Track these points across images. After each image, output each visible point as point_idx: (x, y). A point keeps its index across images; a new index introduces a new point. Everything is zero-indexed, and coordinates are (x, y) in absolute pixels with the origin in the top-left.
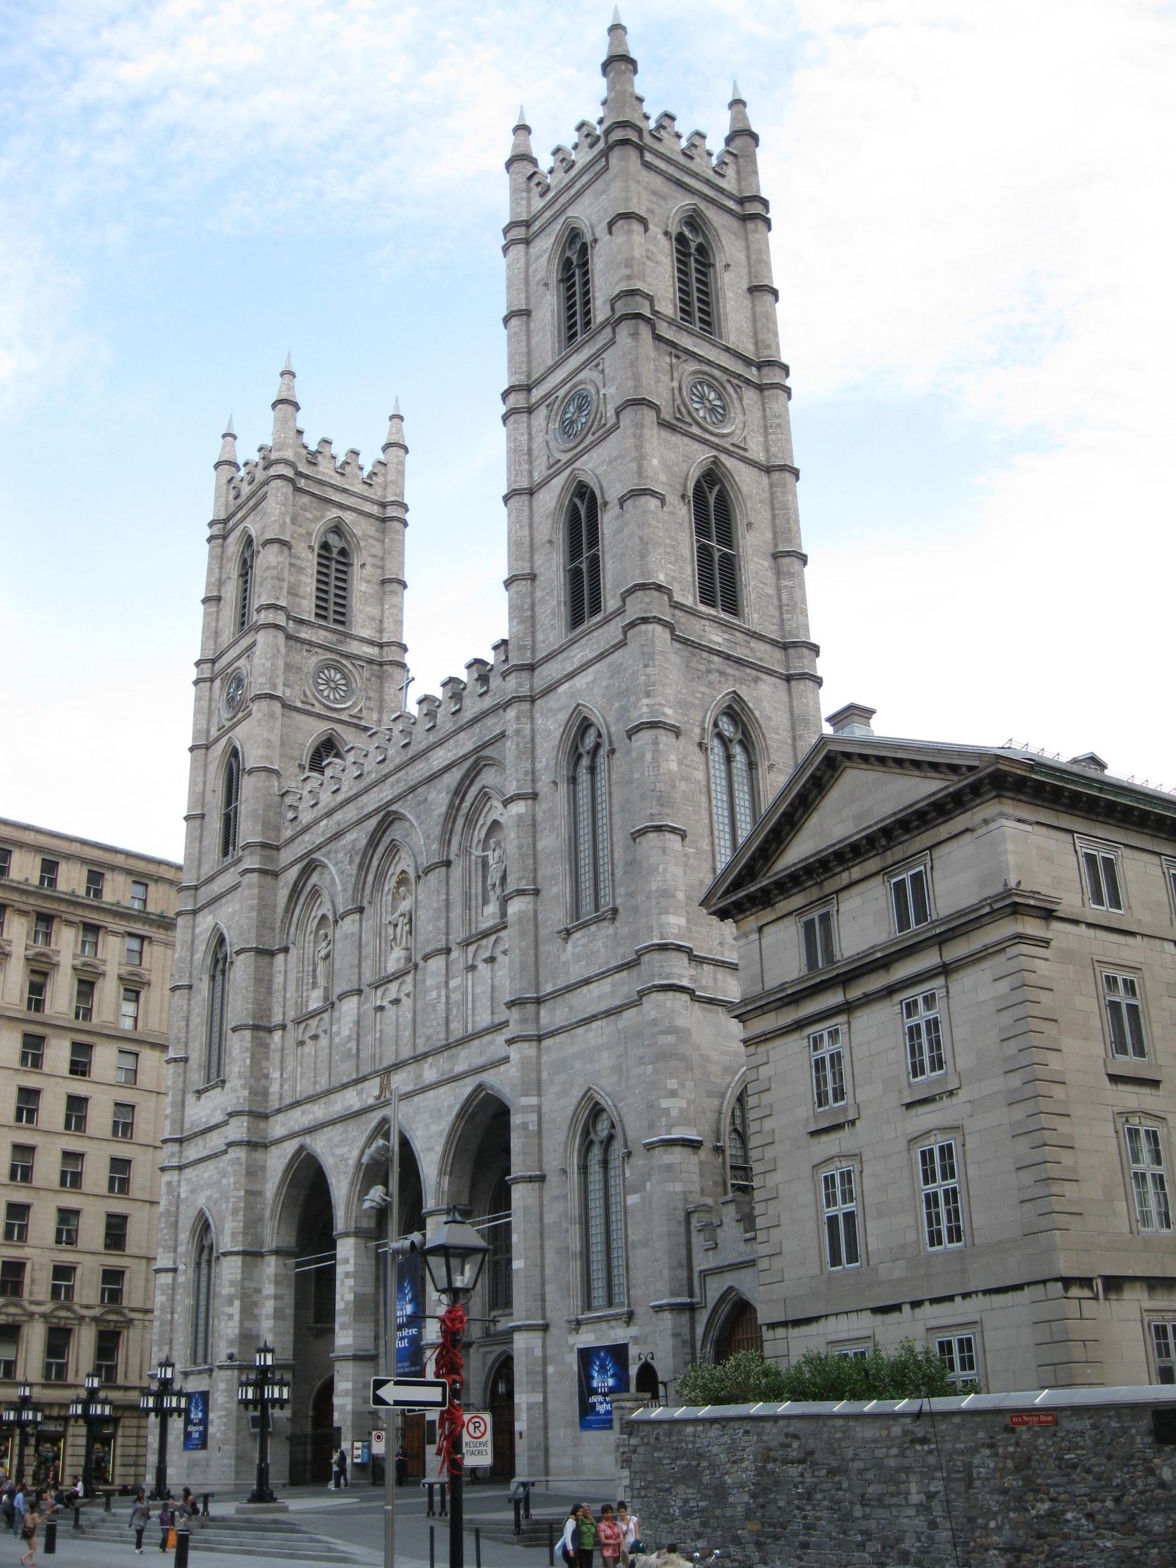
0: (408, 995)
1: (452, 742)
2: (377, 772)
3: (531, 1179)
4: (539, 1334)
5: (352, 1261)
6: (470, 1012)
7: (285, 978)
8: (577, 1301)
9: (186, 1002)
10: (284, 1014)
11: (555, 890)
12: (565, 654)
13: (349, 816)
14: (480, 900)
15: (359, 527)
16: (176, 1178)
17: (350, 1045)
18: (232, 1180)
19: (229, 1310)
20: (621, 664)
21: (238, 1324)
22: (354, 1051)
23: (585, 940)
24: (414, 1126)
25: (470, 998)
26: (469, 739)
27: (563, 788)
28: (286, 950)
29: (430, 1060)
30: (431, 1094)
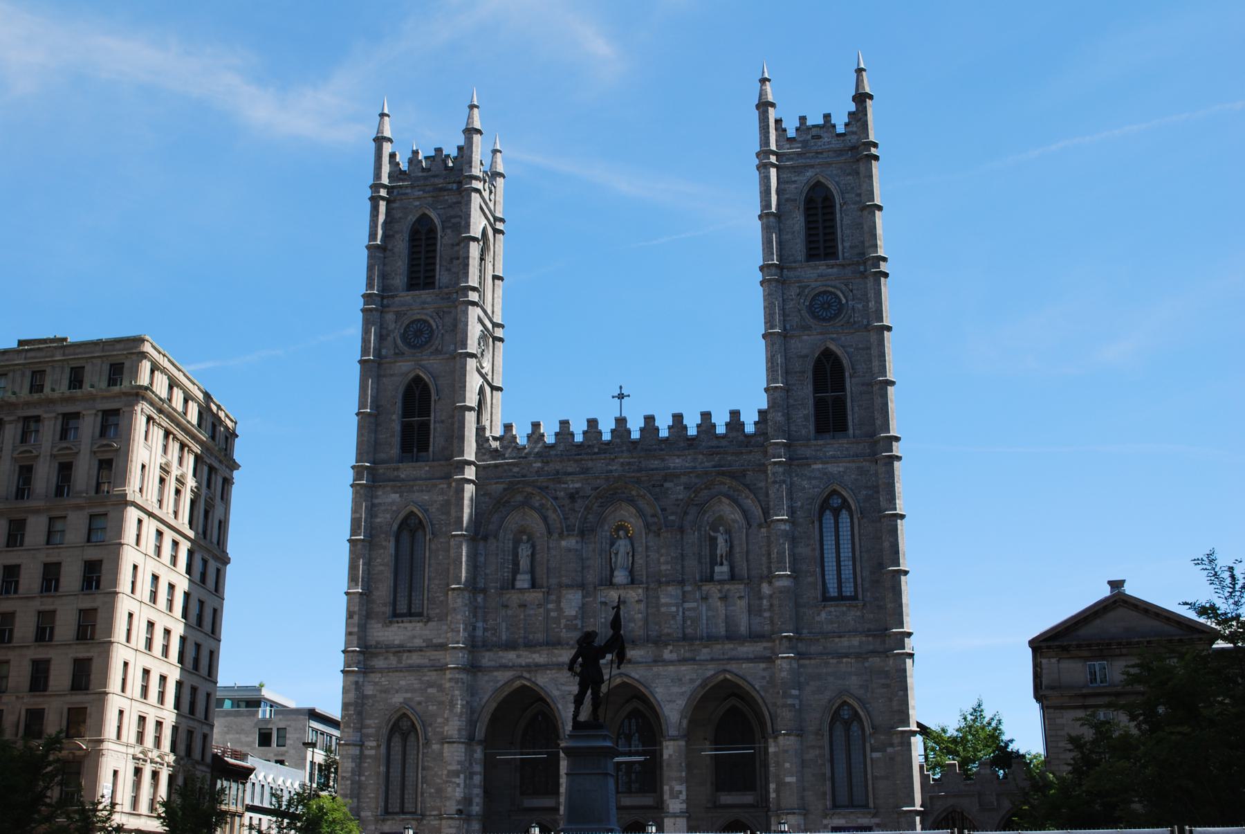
0: (639, 601)
1: (689, 457)
2: (599, 449)
3: (798, 735)
4: (802, 817)
6: (705, 626)
7: (485, 560)
8: (829, 803)
9: (367, 552)
10: (484, 584)
11: (810, 579)
12: (819, 448)
13: (570, 470)
14: (708, 560)
15: (490, 232)
16: (361, 680)
17: (574, 622)
19: (457, 780)
20: (868, 471)
21: (462, 790)
22: (580, 626)
23: (838, 614)
24: (654, 685)
25: (705, 618)
26: (707, 461)
27: (817, 524)
28: (485, 538)
29: (670, 648)
30: (671, 668)
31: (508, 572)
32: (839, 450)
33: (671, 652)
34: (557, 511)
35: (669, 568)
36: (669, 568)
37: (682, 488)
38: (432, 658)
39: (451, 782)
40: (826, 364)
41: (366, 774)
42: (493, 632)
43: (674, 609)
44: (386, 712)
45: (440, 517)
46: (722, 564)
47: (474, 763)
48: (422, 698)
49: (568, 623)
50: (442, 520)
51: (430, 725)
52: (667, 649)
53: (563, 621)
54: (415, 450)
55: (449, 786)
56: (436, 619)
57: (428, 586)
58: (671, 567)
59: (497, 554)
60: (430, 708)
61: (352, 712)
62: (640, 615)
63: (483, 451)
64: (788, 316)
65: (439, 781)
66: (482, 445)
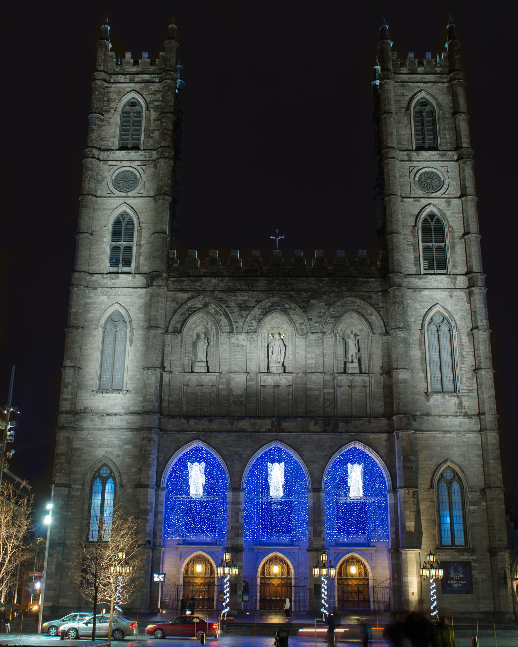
22: (244, 403)
30: (315, 436)
32: (441, 282)
34: (228, 316)
35: (314, 362)
36: (314, 362)
37: (324, 304)
40: (430, 221)
41: (73, 510)
43: (317, 393)
44: (90, 462)
46: (352, 362)
48: (120, 452)
49: (236, 399)
53: (232, 398)
54: (121, 265)
56: (133, 392)
58: (316, 361)
59: (181, 346)
61: (64, 461)
64: (403, 186)
66: (172, 265)
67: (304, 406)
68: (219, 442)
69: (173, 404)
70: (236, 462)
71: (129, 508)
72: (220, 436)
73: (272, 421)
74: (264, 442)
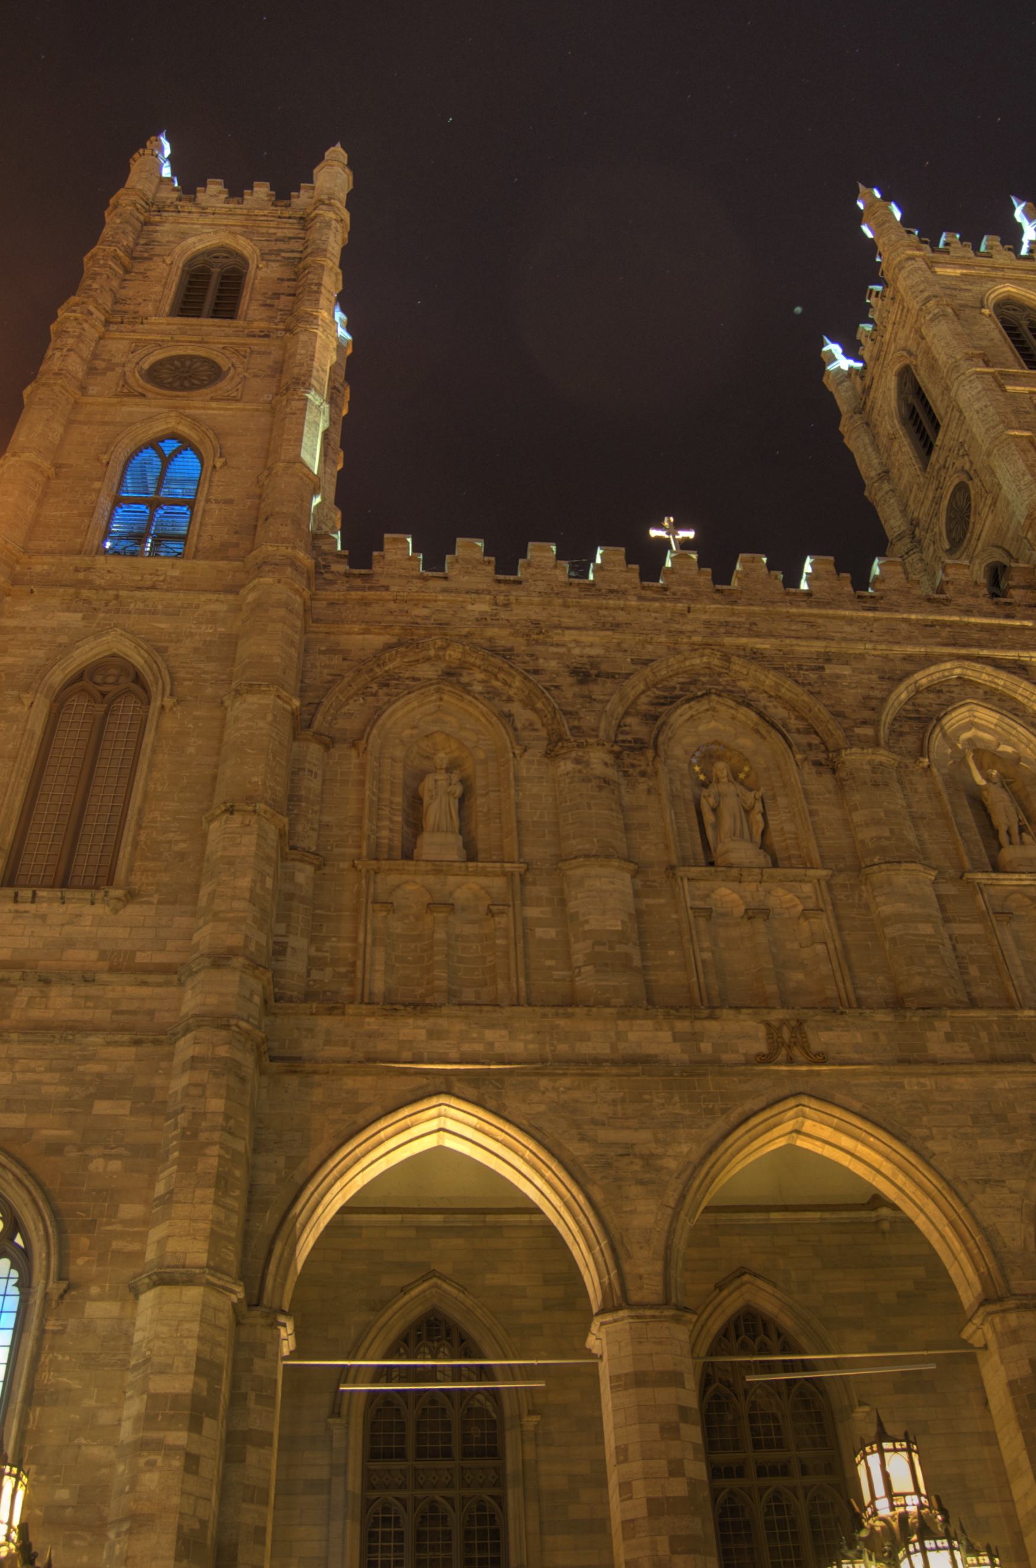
5: (691, 1383)
17: (620, 948)
18: (216, 1105)
30: (963, 1083)
31: (391, 830)
33: (949, 1038)
35: (887, 834)
36: (887, 834)
38: (124, 1006)
39: (158, 1446)
42: (343, 970)
45: (202, 666)
47: (252, 1396)
48: (67, 1133)
49: (598, 949)
50: (205, 672)
51: (89, 1227)
52: (933, 1029)
53: (580, 949)
55: (151, 1464)
56: (155, 899)
57: (141, 811)
59: (362, 783)
60: (97, 1165)
62: (820, 948)
63: (328, 576)
65: (96, 1452)
67: (881, 979)
68: (542, 1108)
69: (329, 970)
70: (634, 1190)
71: (90, 1403)
72: (544, 1082)
73: (768, 1024)
74: (749, 1106)
